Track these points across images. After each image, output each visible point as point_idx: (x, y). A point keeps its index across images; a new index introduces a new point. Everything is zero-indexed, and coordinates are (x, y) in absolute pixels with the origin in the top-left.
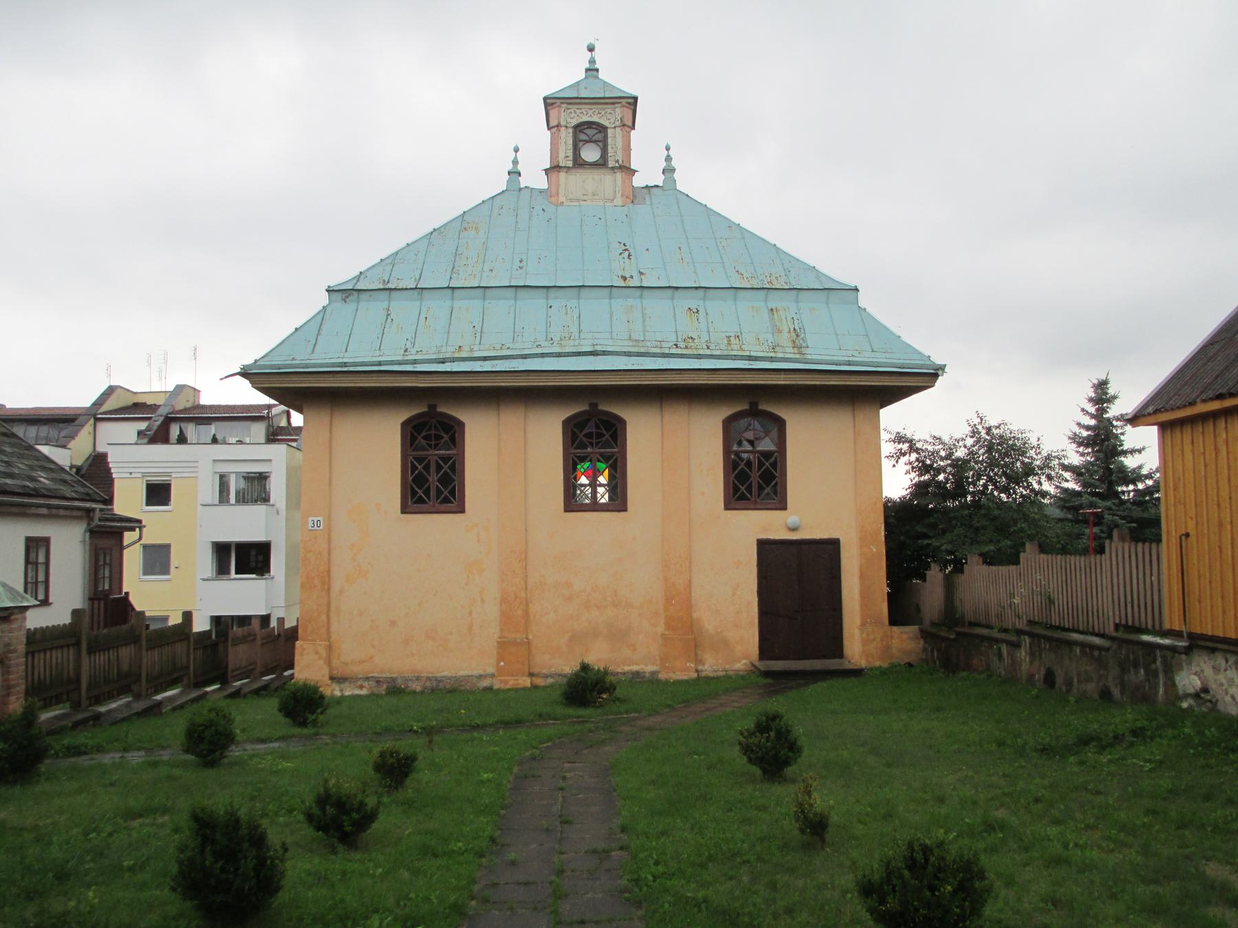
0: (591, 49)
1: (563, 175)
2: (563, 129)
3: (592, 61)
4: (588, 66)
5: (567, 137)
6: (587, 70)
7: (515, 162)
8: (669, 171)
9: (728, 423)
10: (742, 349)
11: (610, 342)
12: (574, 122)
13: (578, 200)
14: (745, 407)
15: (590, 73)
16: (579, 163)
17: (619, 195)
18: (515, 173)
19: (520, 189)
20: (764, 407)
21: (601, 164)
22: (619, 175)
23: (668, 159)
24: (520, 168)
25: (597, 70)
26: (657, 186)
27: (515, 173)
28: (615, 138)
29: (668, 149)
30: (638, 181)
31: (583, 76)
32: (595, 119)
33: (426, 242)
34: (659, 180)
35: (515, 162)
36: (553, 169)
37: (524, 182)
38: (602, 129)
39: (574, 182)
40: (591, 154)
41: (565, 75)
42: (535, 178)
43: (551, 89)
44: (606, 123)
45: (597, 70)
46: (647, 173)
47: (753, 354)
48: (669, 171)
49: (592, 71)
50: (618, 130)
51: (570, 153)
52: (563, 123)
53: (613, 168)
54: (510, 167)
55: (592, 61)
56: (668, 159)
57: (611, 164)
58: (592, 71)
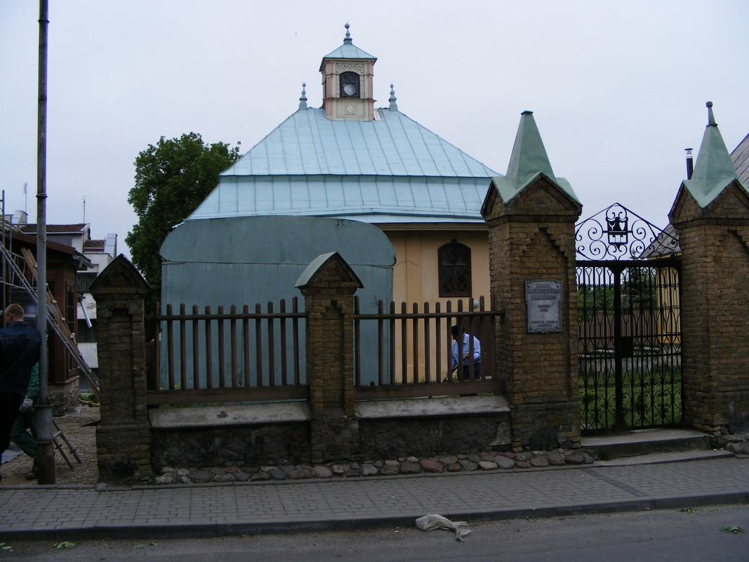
0: (347, 27)
1: (334, 103)
2: (334, 76)
3: (348, 35)
4: (345, 37)
5: (335, 83)
6: (345, 40)
7: (304, 93)
8: (392, 100)
9: (440, 251)
10: (450, 212)
11: (380, 207)
12: (341, 71)
13: (344, 117)
14: (450, 242)
15: (347, 41)
16: (343, 96)
17: (367, 115)
18: (303, 99)
19: (307, 109)
20: (459, 241)
21: (356, 96)
22: (366, 103)
23: (392, 93)
24: (307, 96)
25: (351, 40)
26: (385, 108)
27: (303, 99)
28: (364, 82)
29: (392, 87)
30: (376, 105)
31: (343, 43)
32: (353, 70)
33: (262, 146)
34: (388, 105)
35: (304, 93)
36: (327, 99)
37: (309, 104)
38: (358, 76)
39: (338, 108)
40: (348, 90)
41: (332, 45)
42: (316, 100)
43: (327, 52)
44: (359, 73)
45: (351, 40)
46: (381, 101)
47: (456, 214)
48: (392, 100)
49: (348, 41)
50: (366, 77)
51: (339, 92)
52: (334, 72)
53: (364, 100)
54: (301, 96)
55: (348, 35)
56: (392, 93)
57: (362, 97)
58: (348, 41)
